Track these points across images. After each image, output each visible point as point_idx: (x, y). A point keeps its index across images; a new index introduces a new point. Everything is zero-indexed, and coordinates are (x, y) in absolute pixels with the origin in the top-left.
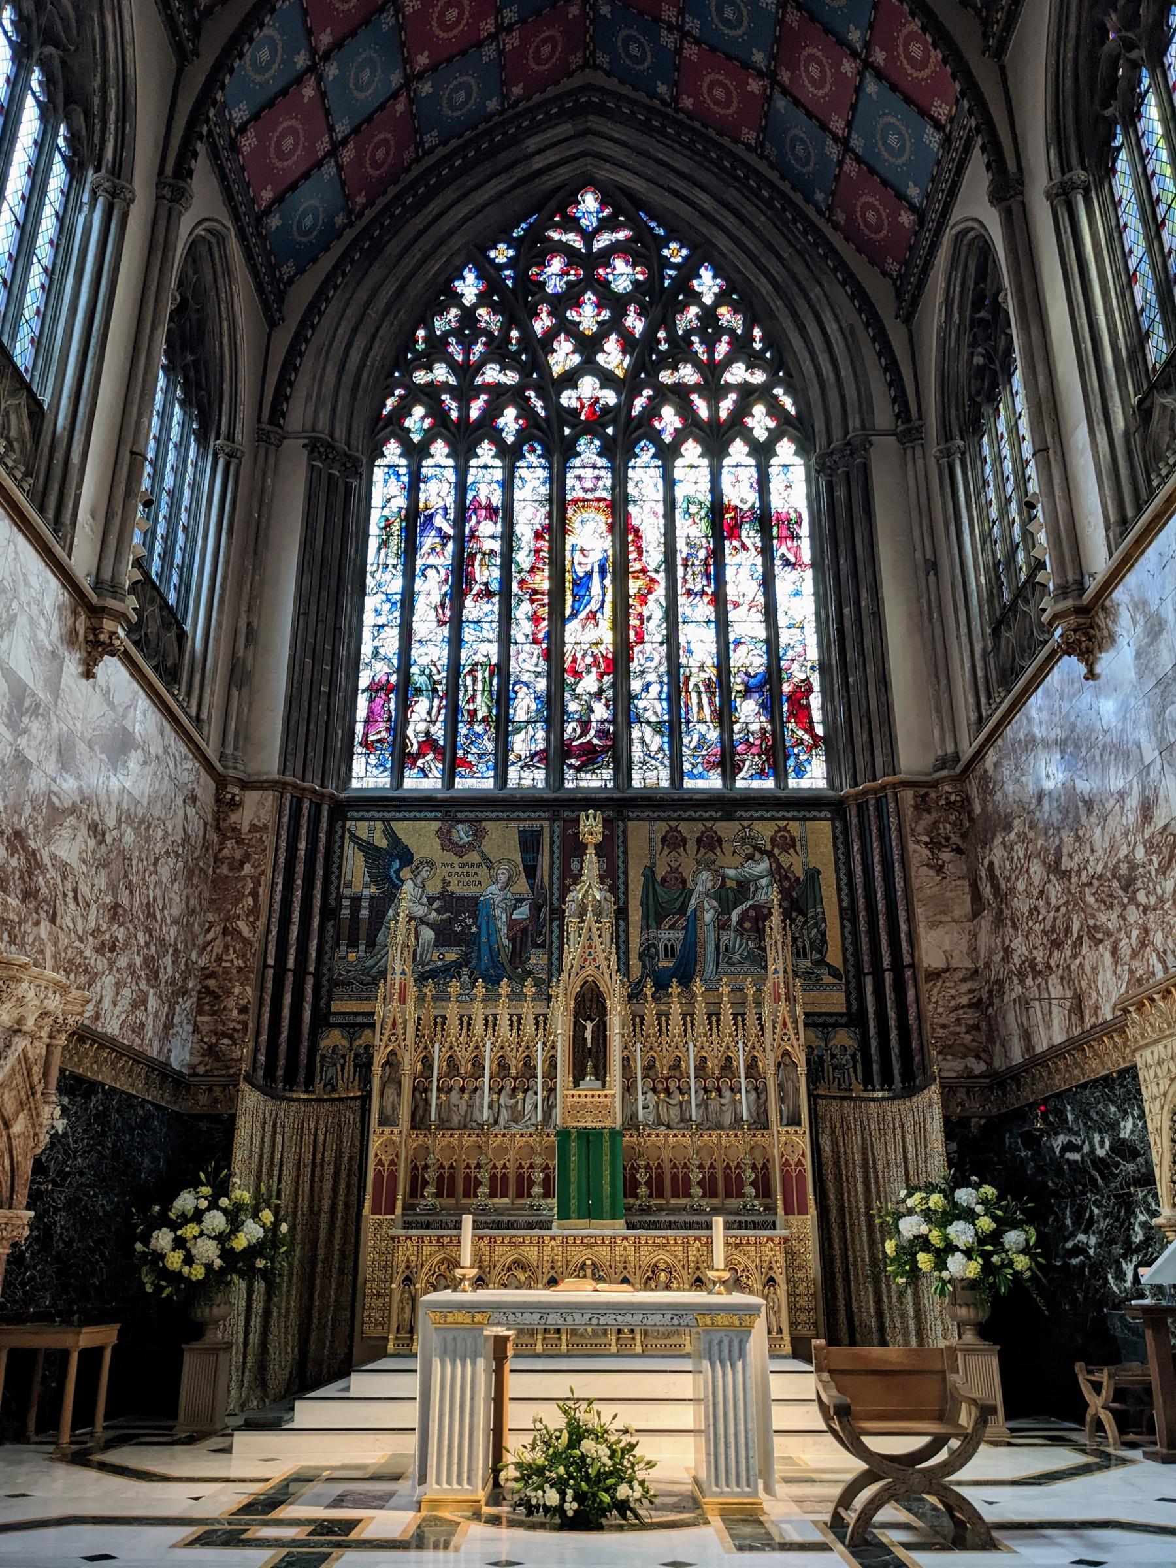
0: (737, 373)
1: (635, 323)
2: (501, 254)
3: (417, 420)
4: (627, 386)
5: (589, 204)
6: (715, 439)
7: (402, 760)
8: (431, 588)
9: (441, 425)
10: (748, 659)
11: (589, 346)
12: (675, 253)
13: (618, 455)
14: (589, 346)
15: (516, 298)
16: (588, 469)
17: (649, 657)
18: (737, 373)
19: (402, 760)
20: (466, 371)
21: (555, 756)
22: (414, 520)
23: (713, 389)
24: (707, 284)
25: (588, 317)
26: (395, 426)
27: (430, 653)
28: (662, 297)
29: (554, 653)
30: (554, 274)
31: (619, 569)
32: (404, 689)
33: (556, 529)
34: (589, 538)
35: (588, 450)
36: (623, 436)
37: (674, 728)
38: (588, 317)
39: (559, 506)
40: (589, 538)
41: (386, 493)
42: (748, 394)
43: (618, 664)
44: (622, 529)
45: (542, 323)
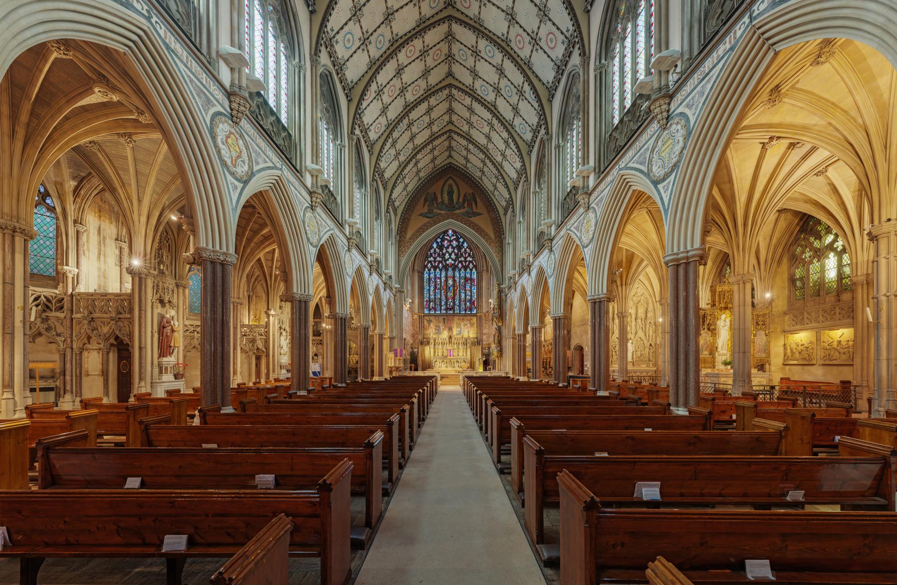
0: (469, 259)
1: (456, 251)
2: (439, 240)
3: (429, 265)
4: (455, 261)
5: (450, 232)
6: (465, 268)
7: (430, 310)
8: (432, 288)
9: (432, 266)
10: (468, 297)
11: (450, 255)
12: (461, 240)
13: (454, 270)
14: (450, 255)
15: (441, 247)
16: (450, 273)
17: (457, 297)
18: (469, 259)
19: (430, 310)
20: (435, 258)
21: (447, 309)
22: (430, 279)
23: (466, 261)
24: (465, 245)
25: (450, 250)
26: (426, 266)
27: (432, 297)
28: (459, 247)
29: (446, 297)
30: (446, 243)
31: (454, 286)
32: (430, 301)
33: (446, 281)
34: (450, 282)
35: (450, 269)
36: (454, 268)
37: (460, 306)
38: (450, 250)
39: (446, 277)
40: (450, 282)
41: (426, 276)
42: (470, 262)
43: (454, 298)
44: (454, 281)
45: (444, 251)
